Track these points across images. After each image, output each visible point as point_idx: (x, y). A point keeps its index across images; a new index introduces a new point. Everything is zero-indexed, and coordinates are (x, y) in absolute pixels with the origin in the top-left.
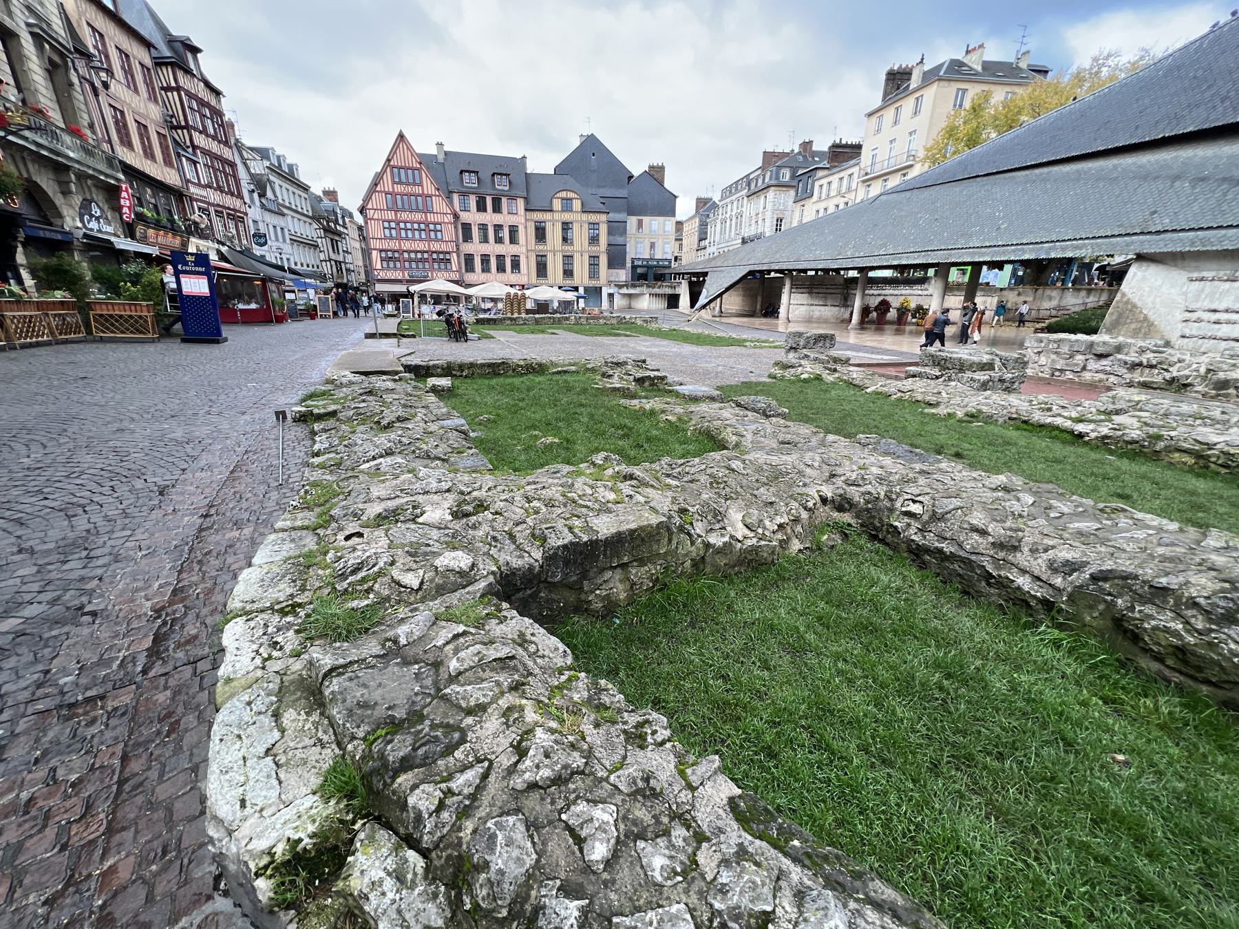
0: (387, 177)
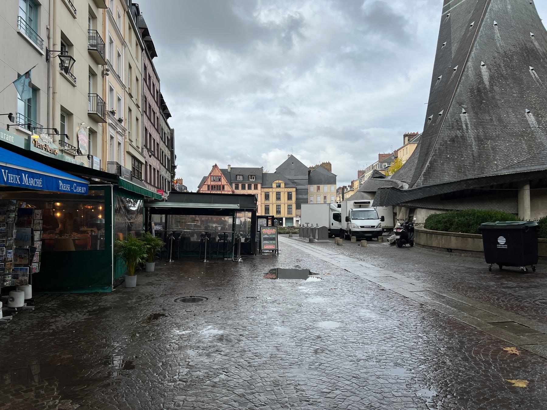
0: (209, 180)
